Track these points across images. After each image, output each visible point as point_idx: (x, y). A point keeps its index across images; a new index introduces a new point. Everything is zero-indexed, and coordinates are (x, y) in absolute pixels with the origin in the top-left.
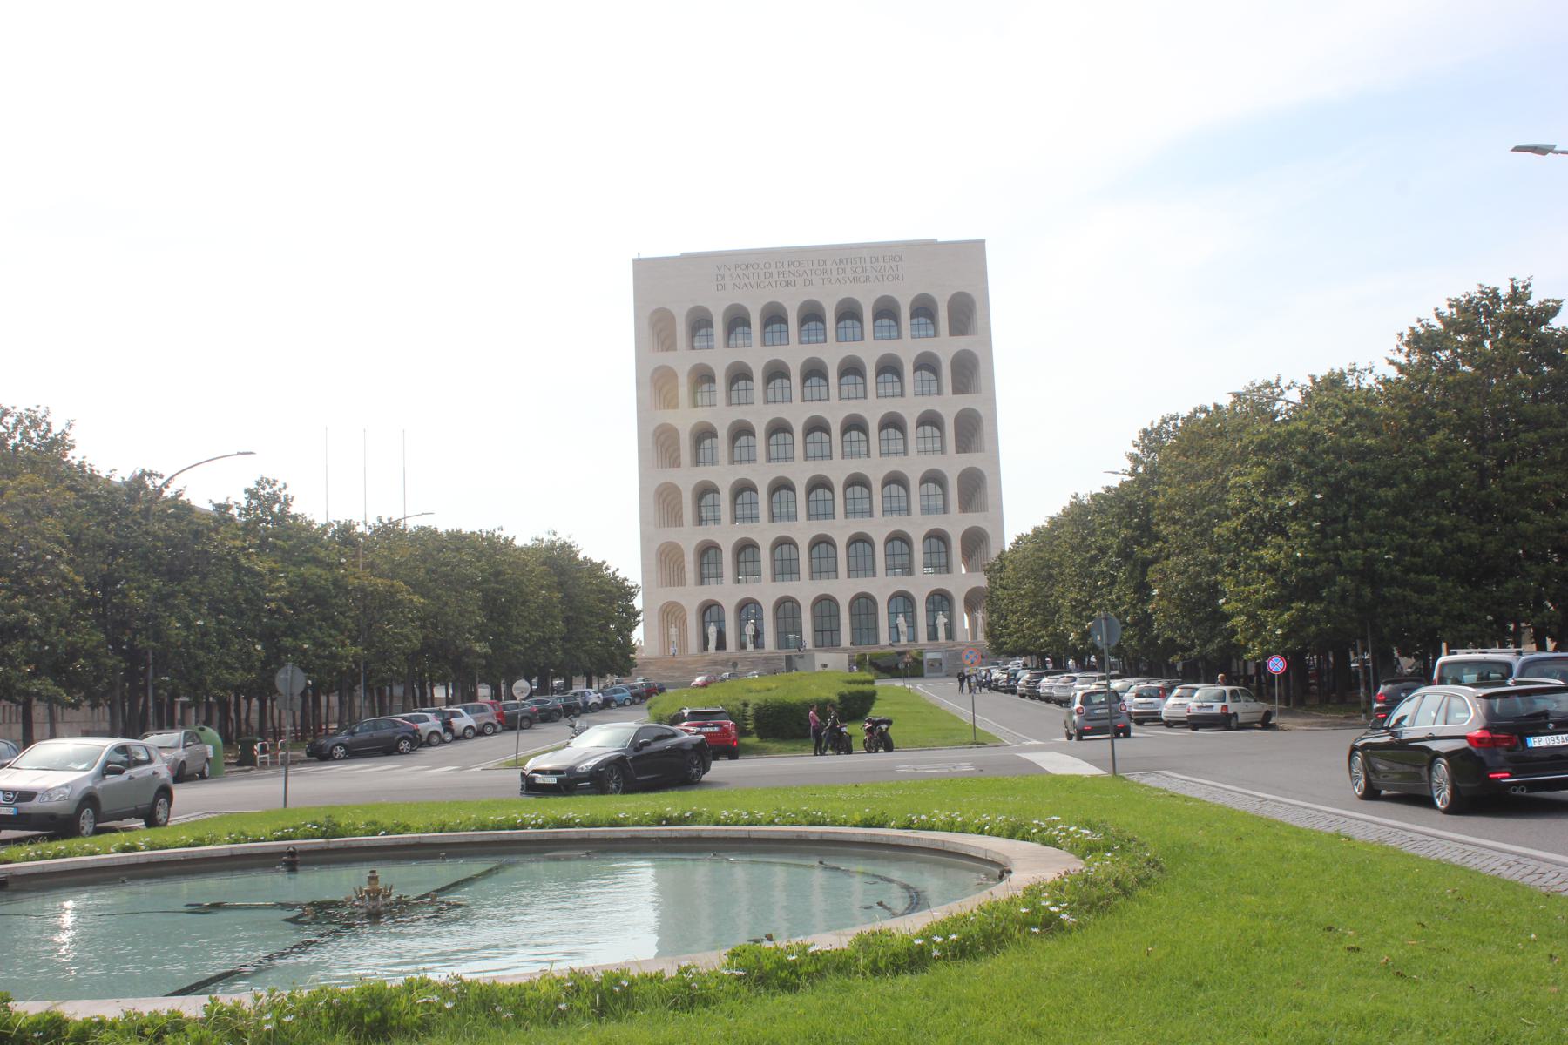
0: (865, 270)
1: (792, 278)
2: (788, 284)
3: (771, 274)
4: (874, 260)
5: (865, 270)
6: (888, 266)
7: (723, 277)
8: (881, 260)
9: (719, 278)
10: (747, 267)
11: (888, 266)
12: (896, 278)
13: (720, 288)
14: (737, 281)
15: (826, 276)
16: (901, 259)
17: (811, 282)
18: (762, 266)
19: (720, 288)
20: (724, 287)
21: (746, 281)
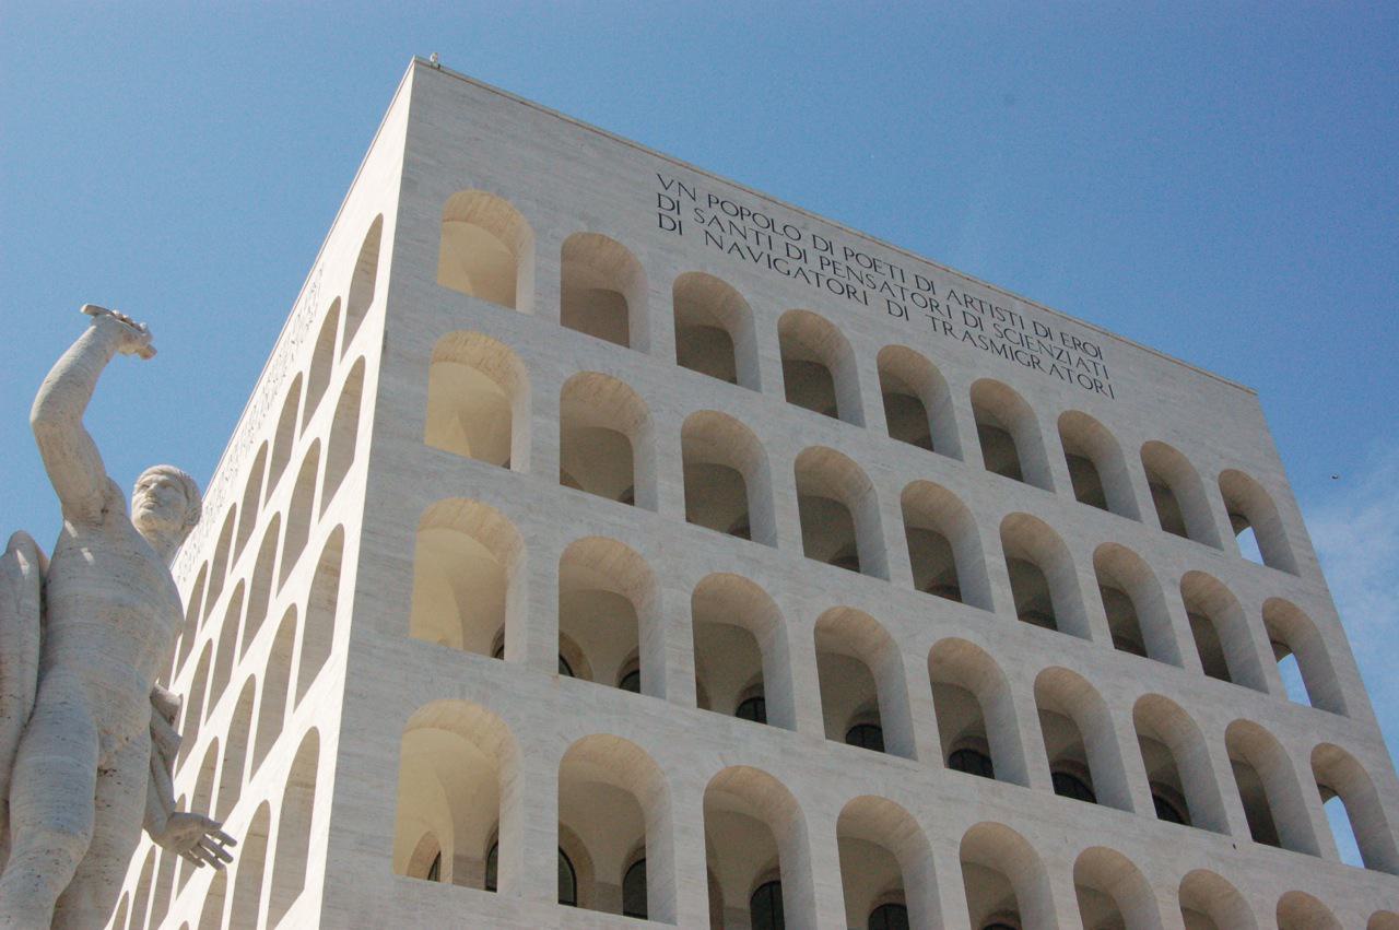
0: (1024, 341)
1: (854, 283)
2: (849, 292)
3: (803, 255)
4: (1041, 331)
5: (1024, 341)
6: (1074, 360)
7: (676, 206)
8: (1055, 332)
9: (667, 204)
10: (740, 212)
11: (1074, 360)
12: (1095, 386)
13: (667, 224)
14: (715, 230)
15: (936, 314)
16: (1098, 353)
17: (904, 313)
18: (779, 229)
19: (667, 224)
20: (678, 227)
21: (741, 242)
